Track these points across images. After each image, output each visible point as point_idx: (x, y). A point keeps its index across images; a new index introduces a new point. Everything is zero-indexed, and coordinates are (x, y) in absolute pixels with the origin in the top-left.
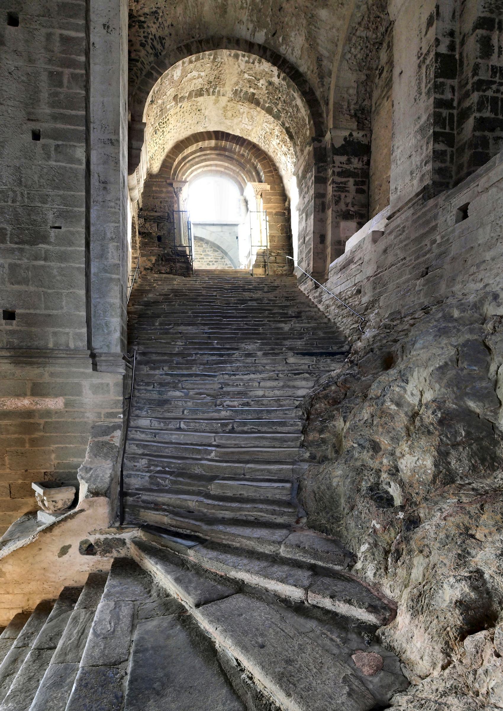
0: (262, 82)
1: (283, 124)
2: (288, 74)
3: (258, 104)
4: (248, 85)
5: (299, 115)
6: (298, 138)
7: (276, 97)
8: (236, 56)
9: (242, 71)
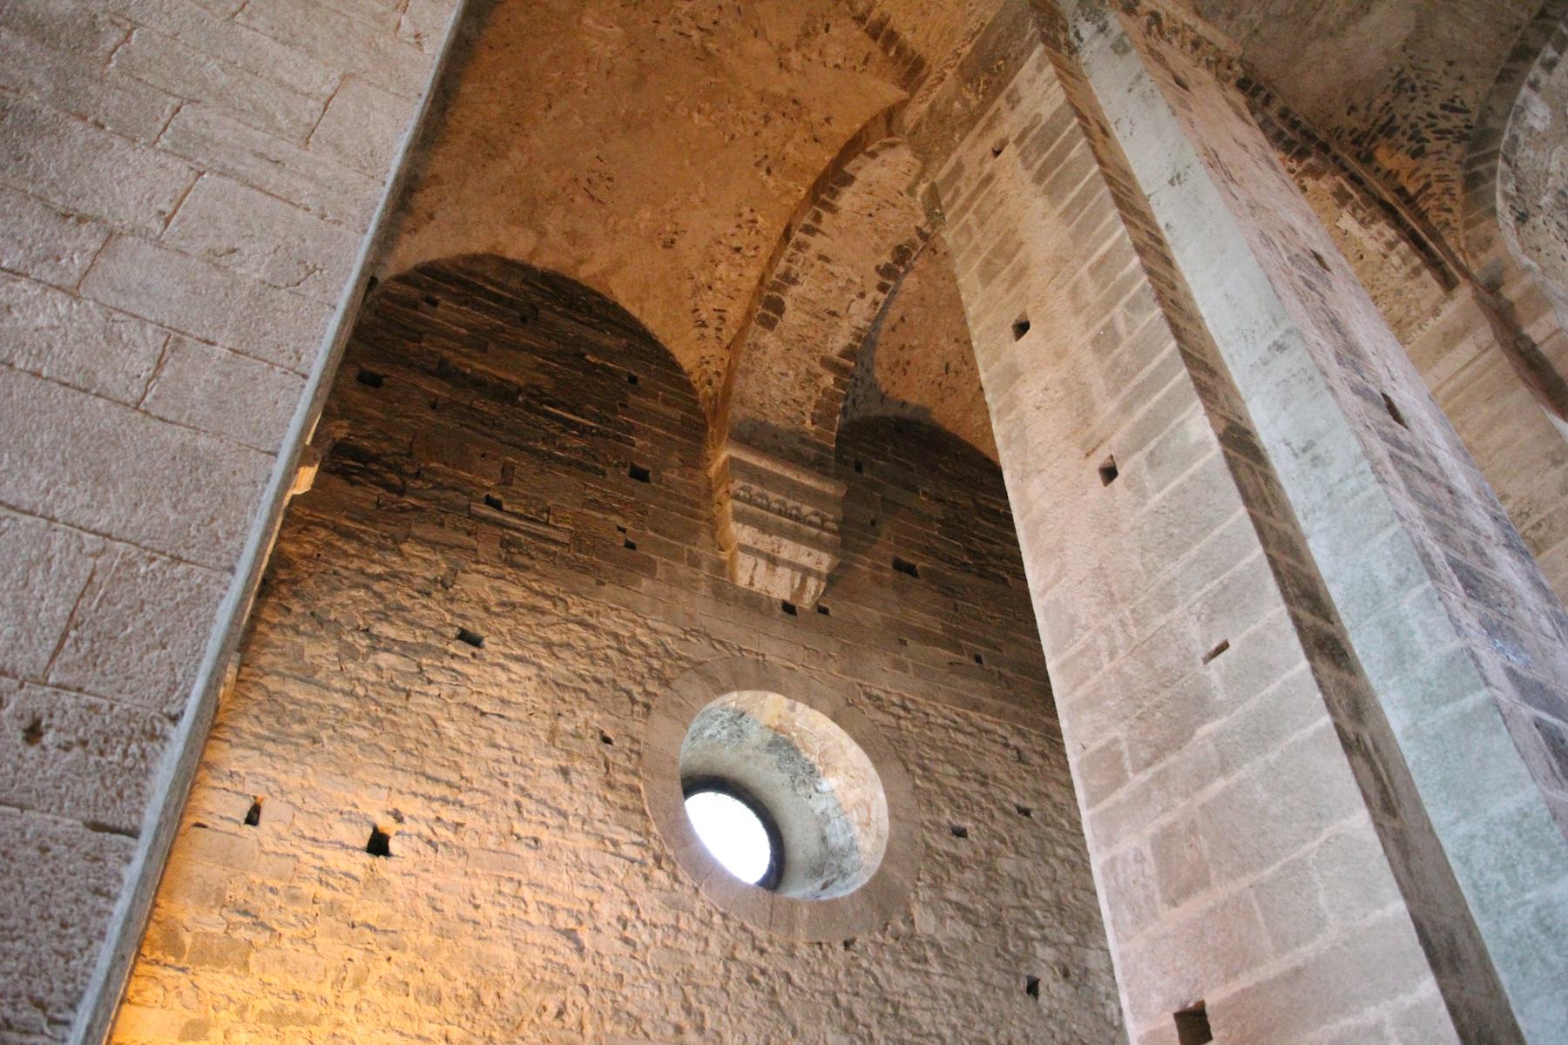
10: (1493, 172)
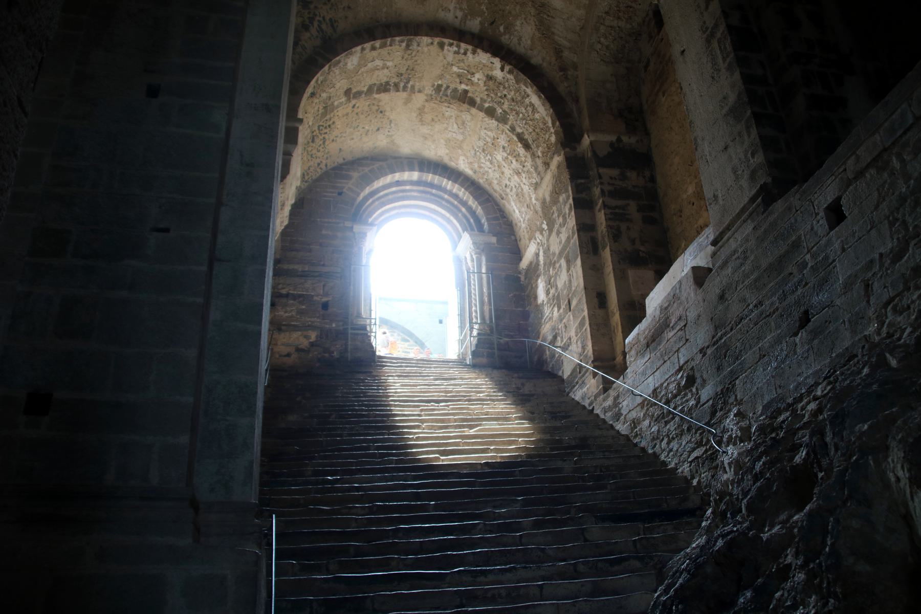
0: (477, 76)
1: (513, 129)
2: (516, 66)
3: (472, 103)
4: (458, 80)
5: (537, 116)
6: (538, 147)
7: (499, 94)
8: (441, 46)
9: (448, 63)
10: (323, 66)
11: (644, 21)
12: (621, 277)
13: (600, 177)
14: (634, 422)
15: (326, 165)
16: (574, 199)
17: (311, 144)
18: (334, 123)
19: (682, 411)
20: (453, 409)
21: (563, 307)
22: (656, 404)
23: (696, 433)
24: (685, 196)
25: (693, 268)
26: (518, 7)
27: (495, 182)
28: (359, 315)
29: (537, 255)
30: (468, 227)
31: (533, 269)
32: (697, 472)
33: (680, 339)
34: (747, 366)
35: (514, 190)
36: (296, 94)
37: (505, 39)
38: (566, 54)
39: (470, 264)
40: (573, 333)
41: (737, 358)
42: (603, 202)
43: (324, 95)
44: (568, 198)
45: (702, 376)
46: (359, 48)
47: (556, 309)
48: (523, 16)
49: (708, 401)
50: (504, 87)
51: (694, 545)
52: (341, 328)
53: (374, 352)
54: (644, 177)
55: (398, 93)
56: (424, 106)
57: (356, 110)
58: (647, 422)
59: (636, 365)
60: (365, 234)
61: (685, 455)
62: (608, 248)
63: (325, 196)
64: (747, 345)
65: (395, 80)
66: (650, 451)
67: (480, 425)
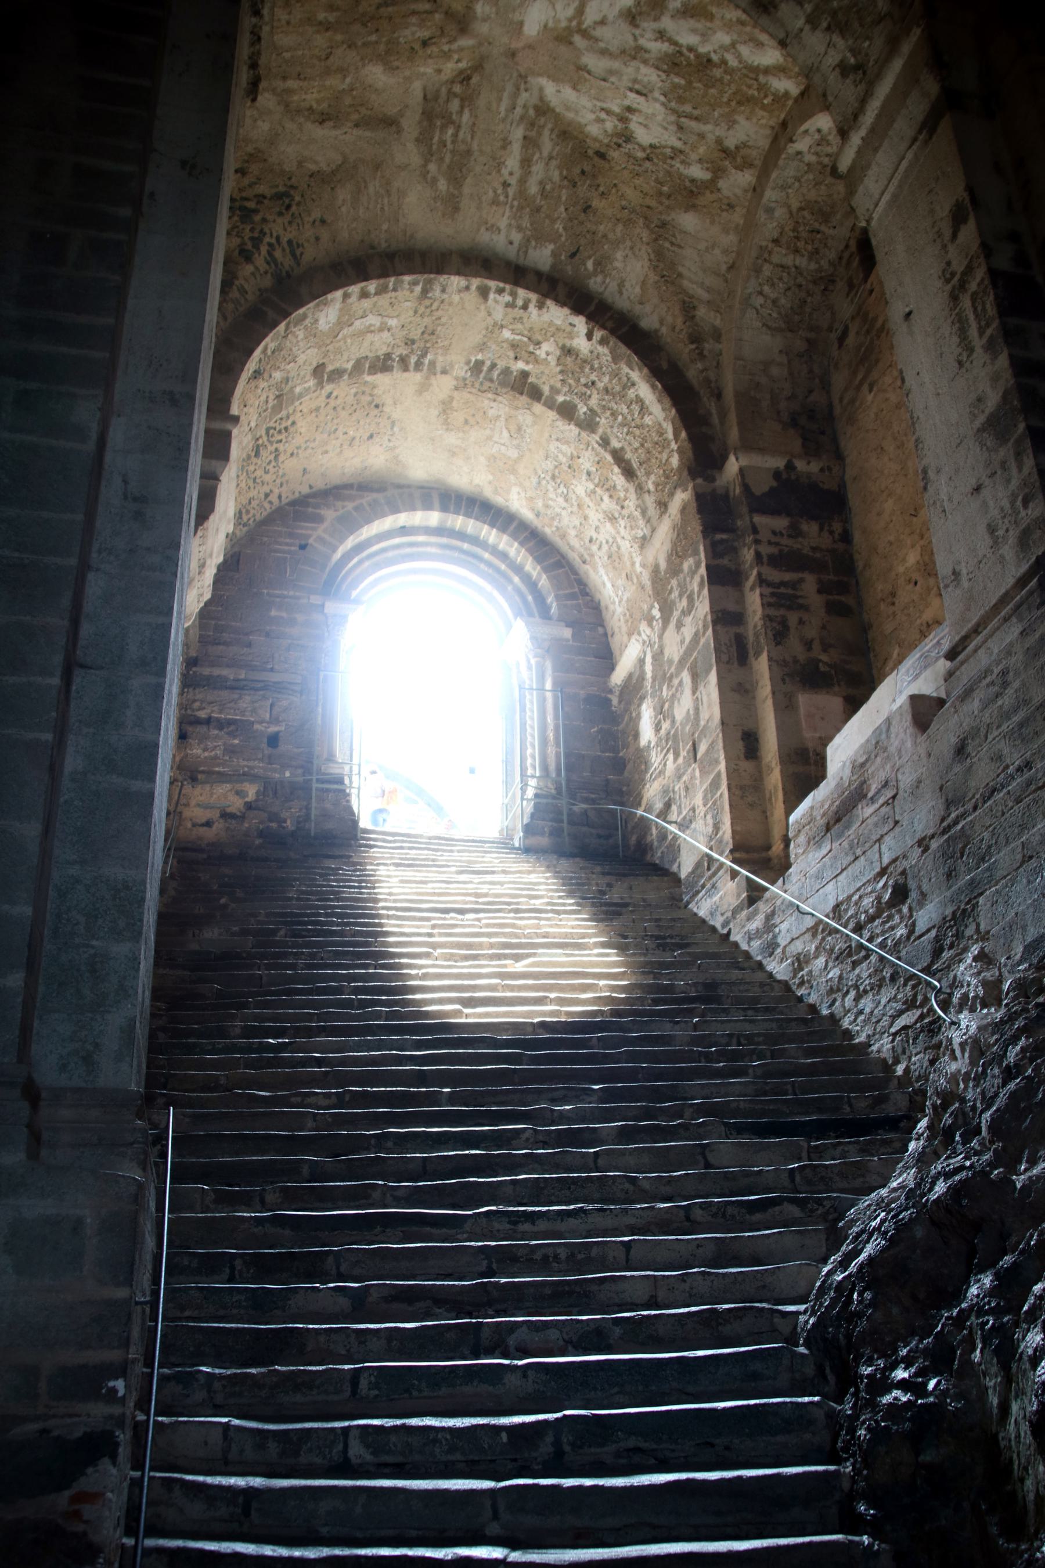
0: (546, 347)
1: (605, 442)
2: (613, 332)
3: (536, 394)
4: (511, 354)
5: (648, 420)
6: (648, 474)
7: (583, 381)
8: (484, 292)
9: (495, 324)
10: (275, 325)
11: (840, 258)
12: (785, 706)
13: (755, 530)
14: (798, 959)
15: (280, 497)
16: (708, 567)
17: (254, 460)
18: (294, 423)
19: (882, 946)
20: (488, 926)
21: (683, 754)
22: (837, 931)
23: (905, 985)
24: (901, 569)
25: (914, 699)
26: (620, 228)
27: (573, 533)
28: (331, 758)
29: (641, 662)
30: (523, 611)
31: (633, 689)
32: (904, 1052)
33: (885, 819)
34: (999, 874)
35: (605, 547)
36: (227, 371)
37: (595, 284)
38: (702, 312)
39: (525, 674)
40: (698, 800)
41: (983, 860)
42: (759, 574)
43: (277, 375)
44: (698, 565)
45: (919, 887)
46: (339, 294)
47: (671, 756)
48: (628, 243)
49: (928, 931)
50: (592, 368)
51: (894, 1184)
52: (301, 779)
53: (355, 823)
54: (831, 533)
55: (406, 374)
56: (452, 398)
57: (332, 403)
58: (821, 961)
59: (806, 861)
60: (345, 617)
61: (885, 1022)
62: (764, 658)
63: (276, 551)
64: (1002, 839)
65: (403, 351)
66: (825, 1012)
67: (534, 955)
